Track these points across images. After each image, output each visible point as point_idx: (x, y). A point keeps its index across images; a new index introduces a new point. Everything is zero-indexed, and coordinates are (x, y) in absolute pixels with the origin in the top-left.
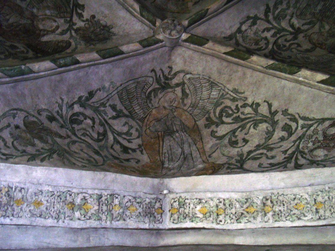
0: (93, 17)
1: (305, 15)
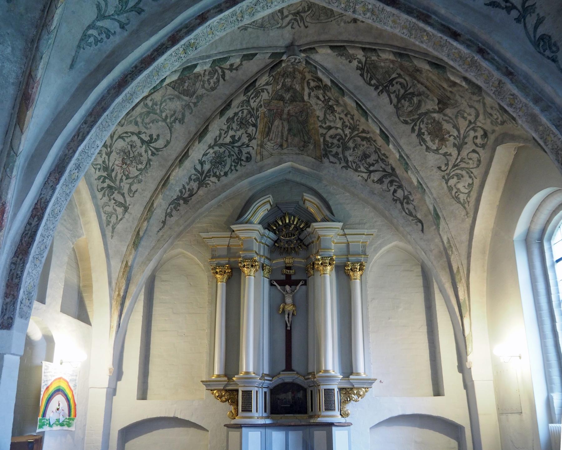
0: (350, 62)
1: (195, 77)
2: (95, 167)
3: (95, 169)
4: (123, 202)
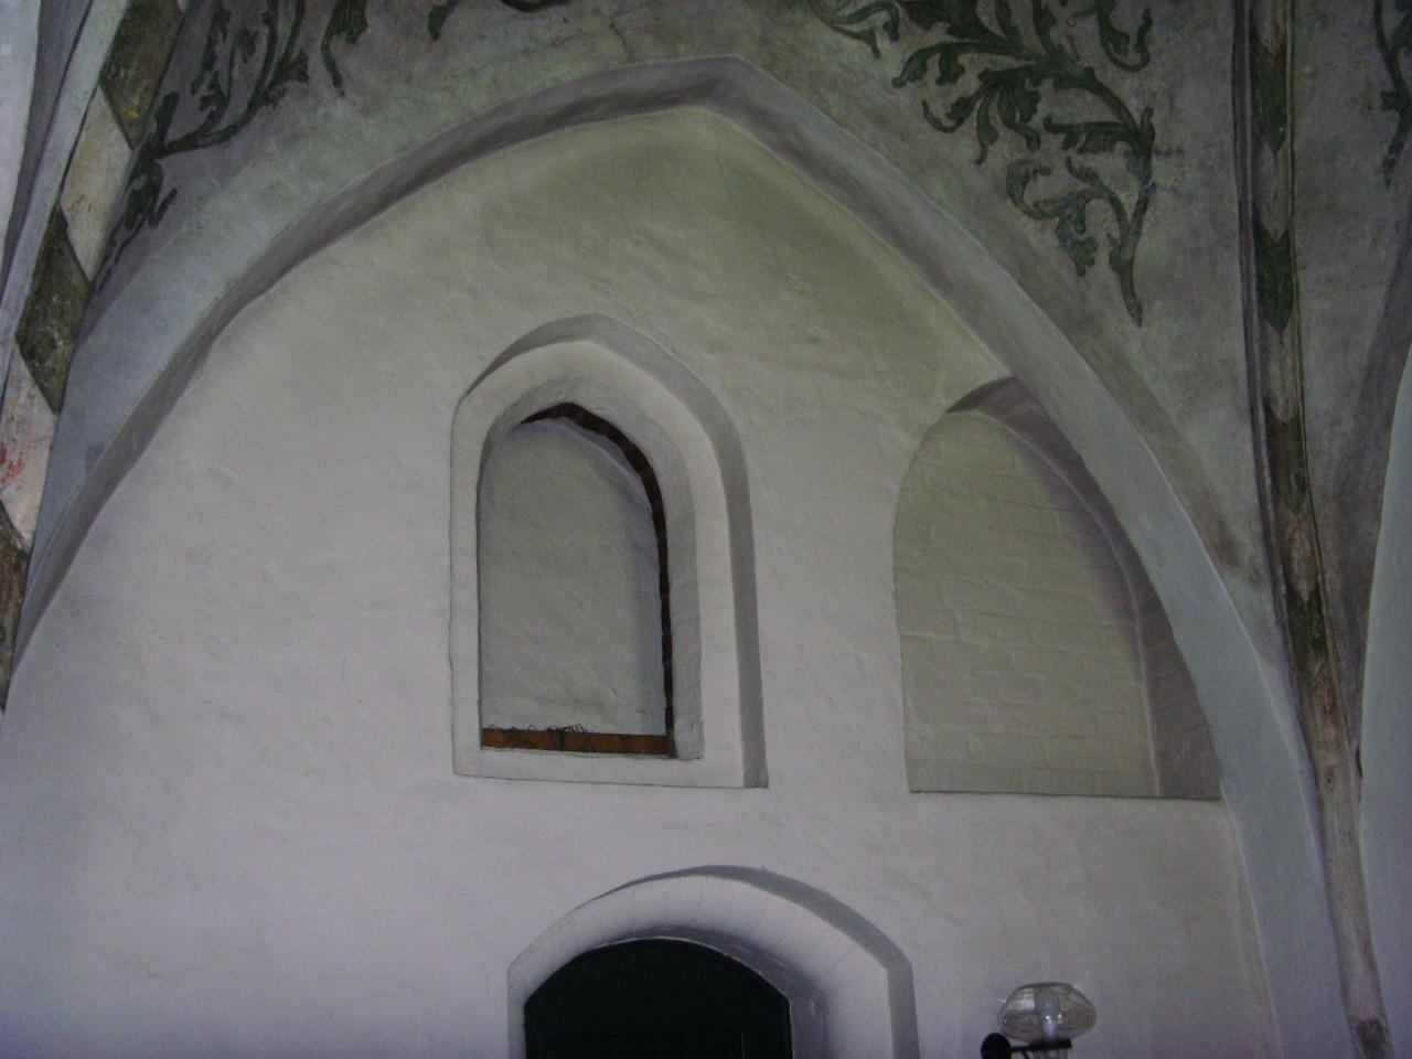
2: (855, 28)
3: (869, 38)
4: (1109, 116)
